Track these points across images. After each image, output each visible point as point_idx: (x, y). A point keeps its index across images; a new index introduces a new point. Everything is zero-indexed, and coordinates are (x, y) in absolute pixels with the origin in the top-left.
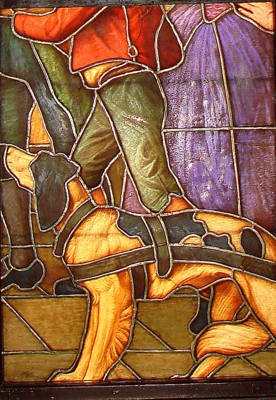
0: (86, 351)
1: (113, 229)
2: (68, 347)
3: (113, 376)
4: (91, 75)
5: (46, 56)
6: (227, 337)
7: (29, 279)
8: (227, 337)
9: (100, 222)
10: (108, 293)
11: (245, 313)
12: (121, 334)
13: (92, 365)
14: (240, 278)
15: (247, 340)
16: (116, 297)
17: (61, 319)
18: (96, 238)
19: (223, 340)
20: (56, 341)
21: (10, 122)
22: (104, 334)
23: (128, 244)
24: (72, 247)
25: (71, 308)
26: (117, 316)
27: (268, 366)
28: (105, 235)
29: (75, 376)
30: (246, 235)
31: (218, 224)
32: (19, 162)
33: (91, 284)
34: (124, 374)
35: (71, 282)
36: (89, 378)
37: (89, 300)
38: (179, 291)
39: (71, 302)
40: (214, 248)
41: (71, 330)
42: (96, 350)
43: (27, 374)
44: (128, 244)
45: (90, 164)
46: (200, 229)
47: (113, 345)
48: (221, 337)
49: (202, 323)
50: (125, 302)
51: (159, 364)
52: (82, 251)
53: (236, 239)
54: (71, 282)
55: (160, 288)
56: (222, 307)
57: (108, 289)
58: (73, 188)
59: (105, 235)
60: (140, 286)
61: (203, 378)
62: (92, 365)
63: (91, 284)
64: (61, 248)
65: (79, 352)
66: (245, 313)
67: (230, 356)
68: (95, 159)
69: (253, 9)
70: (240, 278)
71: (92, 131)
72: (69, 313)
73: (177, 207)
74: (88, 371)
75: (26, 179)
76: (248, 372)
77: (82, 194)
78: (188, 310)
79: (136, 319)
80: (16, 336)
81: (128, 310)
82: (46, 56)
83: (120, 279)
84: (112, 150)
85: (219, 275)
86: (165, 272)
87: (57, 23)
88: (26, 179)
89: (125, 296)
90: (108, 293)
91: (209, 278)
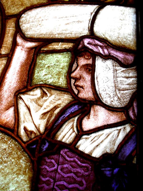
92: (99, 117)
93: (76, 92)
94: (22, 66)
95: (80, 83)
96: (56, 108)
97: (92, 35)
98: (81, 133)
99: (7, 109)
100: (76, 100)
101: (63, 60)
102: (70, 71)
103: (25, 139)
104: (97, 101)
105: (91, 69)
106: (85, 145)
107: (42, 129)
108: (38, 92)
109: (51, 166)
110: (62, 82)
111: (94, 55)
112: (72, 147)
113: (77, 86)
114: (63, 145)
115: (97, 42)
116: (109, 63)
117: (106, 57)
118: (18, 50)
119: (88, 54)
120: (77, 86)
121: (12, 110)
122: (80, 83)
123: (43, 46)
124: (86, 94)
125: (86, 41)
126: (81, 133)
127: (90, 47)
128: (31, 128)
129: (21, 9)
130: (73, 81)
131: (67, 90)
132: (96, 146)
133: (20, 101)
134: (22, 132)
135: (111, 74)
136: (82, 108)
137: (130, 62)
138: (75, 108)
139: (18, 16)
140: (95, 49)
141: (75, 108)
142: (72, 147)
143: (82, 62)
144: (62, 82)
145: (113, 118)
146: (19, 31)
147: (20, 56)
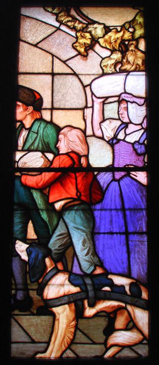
0: (52, 343)
1: (67, 282)
2: (43, 340)
3: (65, 355)
4: (58, 206)
5: (37, 196)
6: (122, 337)
7: (27, 306)
8: (122, 337)
9: (61, 278)
10: (64, 314)
11: (131, 325)
12: (69, 335)
13: (55, 350)
14: (129, 308)
15: (132, 339)
16: (67, 316)
17: (40, 326)
18: (58, 286)
19: (120, 339)
20: (36, 337)
21: (17, 228)
22: (61, 335)
23: (75, 290)
24: (46, 291)
25: (45, 321)
26: (68, 326)
27: (143, 351)
28: (62, 285)
29: (47, 355)
30: (131, 285)
31: (118, 280)
32: (21, 248)
33: (55, 310)
34: (69, 354)
35: (46, 308)
36: (53, 356)
37: (53, 315)
38: (96, 315)
39: (45, 319)
40: (118, 292)
41: (45, 332)
42: (57, 343)
43: (23, 354)
44: (75, 290)
45: (55, 250)
46: (111, 284)
47: (65, 340)
48: (119, 337)
49: (110, 330)
50: (72, 319)
51: (87, 351)
52: (51, 292)
53: (127, 289)
54: (46, 308)
55: (89, 312)
56: (120, 322)
57: (64, 312)
58: (47, 260)
59: (62, 285)
60: (79, 314)
61: (109, 357)
62: (55, 350)
63: (55, 310)
64: (41, 291)
65: (48, 343)
66: (131, 325)
67: (123, 347)
68: (59, 247)
69: (137, 175)
70: (129, 308)
71: (57, 233)
72: (43, 323)
73: (99, 271)
74: (53, 352)
75: (25, 257)
76: (131, 354)
77: (52, 265)
78: (103, 322)
79: (76, 327)
80: (17, 334)
81: (73, 323)
82: (37, 196)
83: (70, 307)
84: (69, 244)
85: (118, 306)
86: (92, 305)
87: (42, 180)
88: (25, 257)
89: (72, 315)
90: (64, 314)
91: (114, 307)
92: (131, 128)
93: (122, 120)
94: (99, 111)
95: (123, 116)
96: (116, 127)
97: (125, 92)
98: (126, 135)
99: (98, 130)
100: (123, 123)
101: (116, 105)
102: (118, 112)
103: (107, 140)
104: (131, 122)
105: (127, 109)
106: (128, 139)
107: (113, 136)
108: (108, 122)
109: (117, 147)
110: (117, 117)
111: (127, 102)
112: (124, 140)
113: (122, 117)
114: (120, 140)
115: (128, 95)
116: (134, 105)
117: (132, 102)
118: (95, 104)
119: (125, 102)
120: (122, 117)
121: (100, 130)
122: (123, 116)
123: (105, 100)
124: (126, 120)
125: (123, 96)
126: (126, 135)
127: (125, 98)
128: (108, 135)
129: (91, 81)
130: (120, 115)
131: (119, 119)
132: (131, 139)
133: (102, 126)
134: (105, 138)
135: (134, 111)
136: (125, 125)
137: (142, 103)
138: (123, 126)
139: (90, 85)
140: (127, 99)
141: (123, 126)
142: (124, 140)
143: (123, 105)
144: (117, 117)
145: (139, 127)
146: (93, 94)
147: (97, 107)
